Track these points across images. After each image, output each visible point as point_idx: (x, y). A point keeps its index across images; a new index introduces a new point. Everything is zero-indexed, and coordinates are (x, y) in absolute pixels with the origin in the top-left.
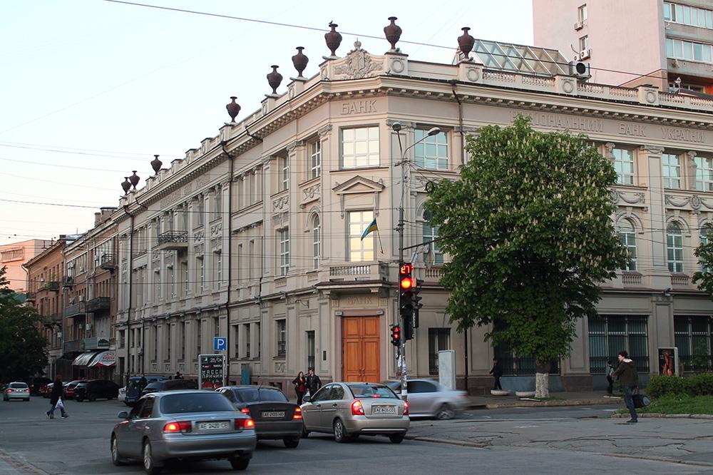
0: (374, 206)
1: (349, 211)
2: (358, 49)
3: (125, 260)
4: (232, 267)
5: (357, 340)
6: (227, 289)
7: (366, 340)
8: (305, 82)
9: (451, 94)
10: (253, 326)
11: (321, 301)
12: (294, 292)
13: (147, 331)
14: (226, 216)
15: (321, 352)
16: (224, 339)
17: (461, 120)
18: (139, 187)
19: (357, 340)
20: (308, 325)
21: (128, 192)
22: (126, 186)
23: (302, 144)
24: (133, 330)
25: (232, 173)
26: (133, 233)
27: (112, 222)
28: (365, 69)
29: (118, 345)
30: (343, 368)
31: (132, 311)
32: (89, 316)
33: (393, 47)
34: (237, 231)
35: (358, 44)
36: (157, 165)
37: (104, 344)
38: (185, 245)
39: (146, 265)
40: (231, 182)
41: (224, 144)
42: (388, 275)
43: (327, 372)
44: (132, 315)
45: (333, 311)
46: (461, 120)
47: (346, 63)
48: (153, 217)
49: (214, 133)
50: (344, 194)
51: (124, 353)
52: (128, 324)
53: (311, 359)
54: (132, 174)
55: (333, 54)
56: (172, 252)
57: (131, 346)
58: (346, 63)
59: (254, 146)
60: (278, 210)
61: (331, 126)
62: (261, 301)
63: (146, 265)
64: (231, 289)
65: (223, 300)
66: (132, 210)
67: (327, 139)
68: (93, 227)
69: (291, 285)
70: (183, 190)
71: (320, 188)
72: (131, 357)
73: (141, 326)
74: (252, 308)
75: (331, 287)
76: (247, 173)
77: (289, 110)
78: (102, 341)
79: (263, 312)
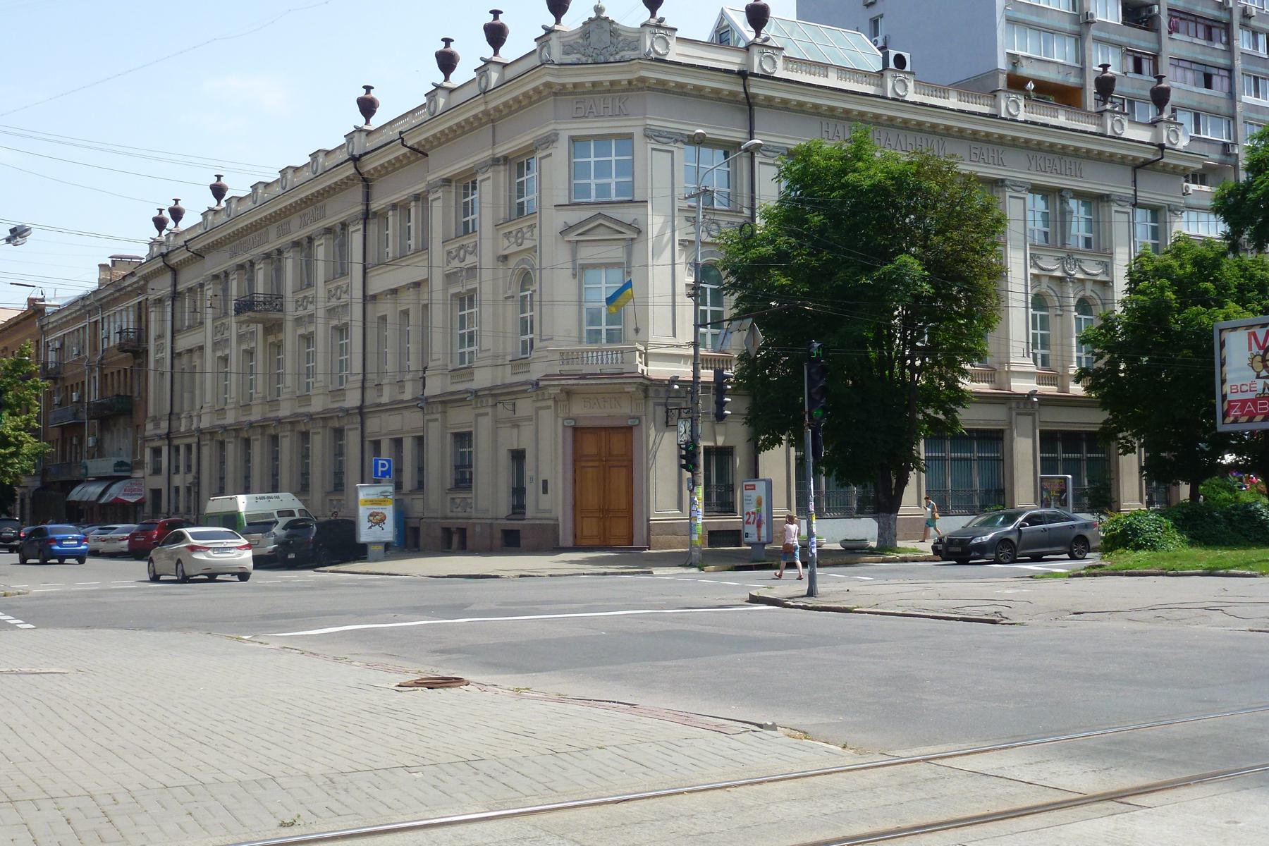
0: (624, 260)
1: (584, 267)
2: (599, 22)
3: (160, 337)
4: (369, 349)
5: (596, 464)
6: (359, 384)
8: (505, 66)
9: (739, 92)
10: (408, 445)
11: (540, 404)
12: (490, 389)
13: (205, 451)
14: (357, 270)
15: (537, 479)
16: (389, 461)
18: (184, 224)
19: (596, 464)
20: (510, 439)
21: (165, 232)
22: (160, 223)
23: (502, 162)
24: (177, 449)
25: (367, 205)
26: (175, 296)
27: (135, 279)
28: (612, 49)
29: (148, 469)
30: (575, 505)
31: (173, 417)
32: (91, 426)
33: (653, 15)
34: (374, 297)
35: (598, 10)
36: (218, 191)
37: (124, 468)
38: (277, 315)
39: (201, 348)
40: (367, 216)
41: (355, 159)
42: (646, 365)
43: (550, 511)
44: (175, 423)
45: (560, 420)
47: (581, 37)
48: (215, 271)
49: (333, 139)
50: (577, 241)
51: (160, 482)
52: (169, 437)
53: (518, 491)
54: (172, 204)
55: (558, 22)
56: (253, 327)
57: (173, 470)
58: (581, 37)
59: (410, 163)
60: (456, 264)
61: (557, 135)
62: (423, 403)
63: (201, 348)
64: (368, 384)
65: (353, 400)
66: (174, 260)
67: (550, 155)
68: (95, 286)
69: (483, 378)
70: (273, 231)
71: (536, 231)
72: (173, 490)
73: (194, 441)
74: (407, 413)
75: (563, 382)
76: (394, 207)
77: (482, 108)
78: (120, 464)
79: (429, 421)
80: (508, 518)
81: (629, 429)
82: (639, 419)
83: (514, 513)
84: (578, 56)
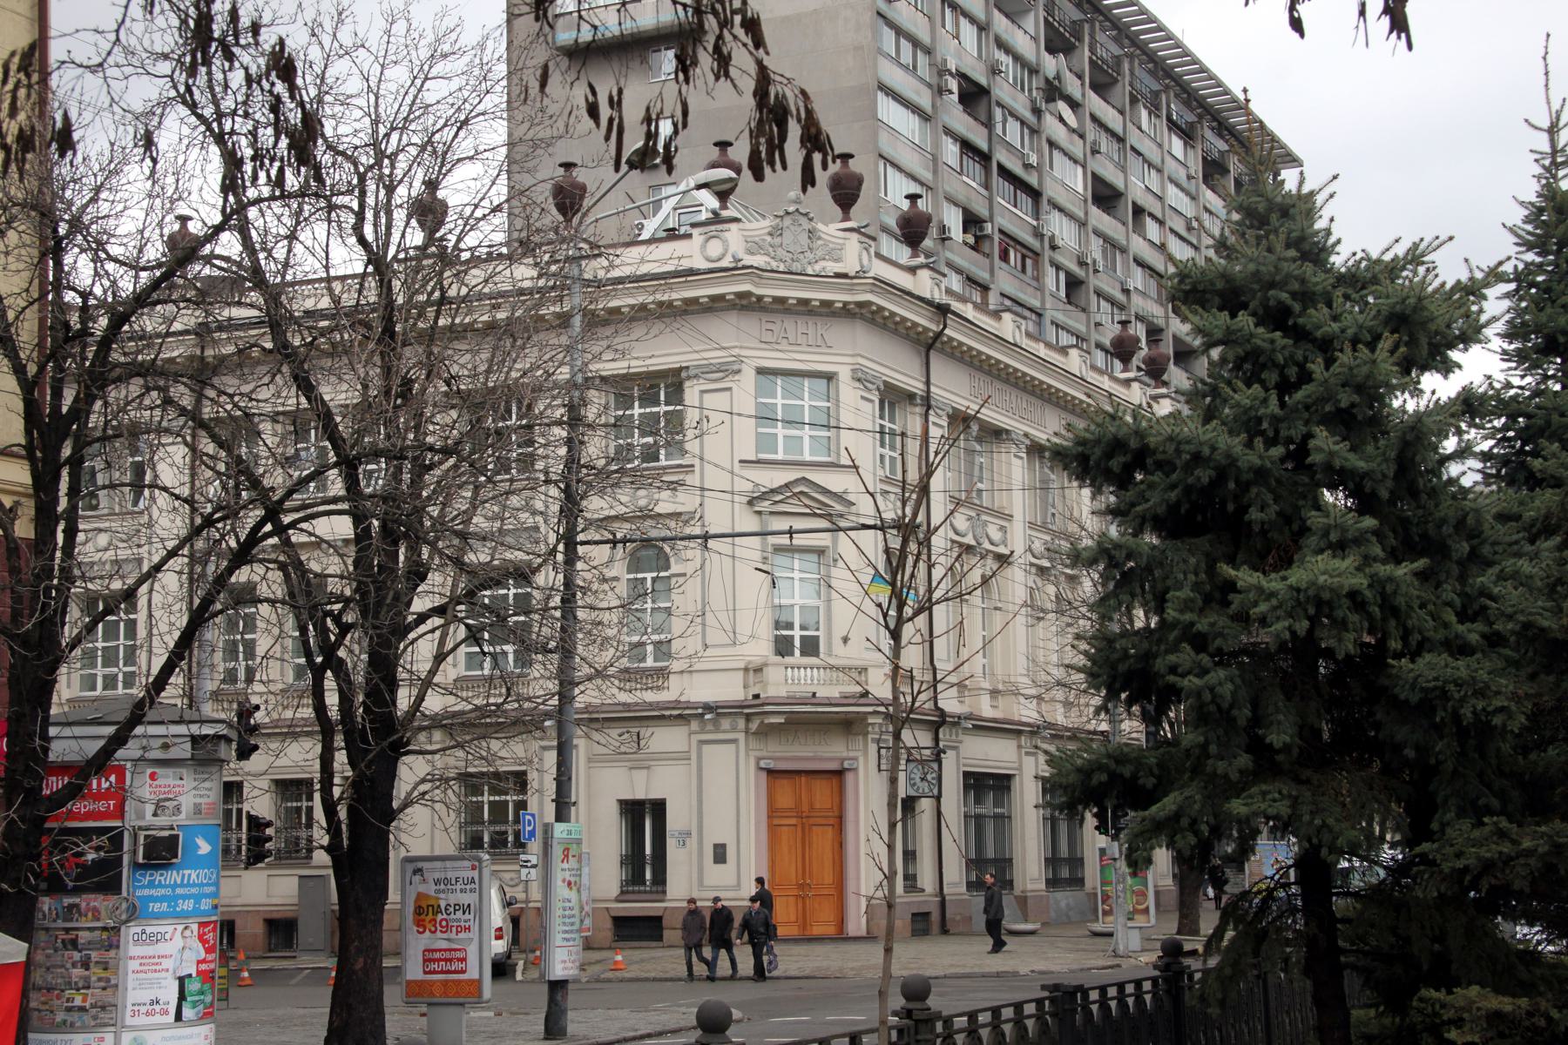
5: (793, 821)
7: (812, 821)
17: (928, 383)
19: (793, 821)
46: (928, 383)
50: (772, 513)
80: (617, 900)
81: (839, 774)
82: (855, 759)
83: (622, 892)
84: (767, 259)
